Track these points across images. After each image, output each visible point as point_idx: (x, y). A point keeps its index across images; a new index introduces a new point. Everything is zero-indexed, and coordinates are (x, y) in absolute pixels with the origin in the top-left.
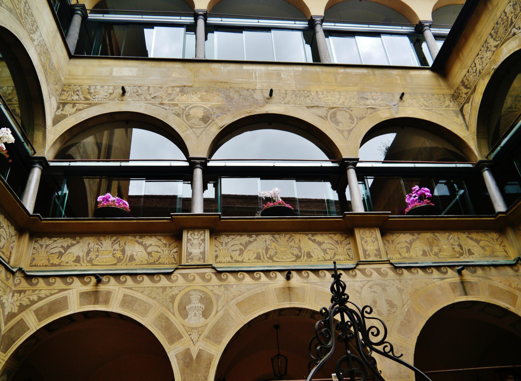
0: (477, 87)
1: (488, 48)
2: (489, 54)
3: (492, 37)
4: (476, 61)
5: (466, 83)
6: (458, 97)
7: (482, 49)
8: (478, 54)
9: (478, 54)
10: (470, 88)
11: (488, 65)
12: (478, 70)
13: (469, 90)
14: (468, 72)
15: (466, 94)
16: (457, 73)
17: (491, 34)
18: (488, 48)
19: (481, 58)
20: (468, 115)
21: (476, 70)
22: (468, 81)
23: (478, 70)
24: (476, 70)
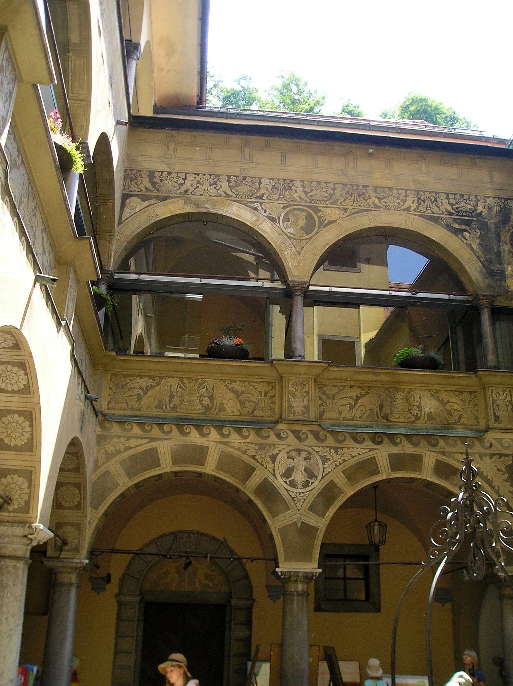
0: (170, 200)
1: (215, 183)
2: (212, 191)
3: (229, 181)
4: (190, 177)
5: (157, 180)
6: (131, 180)
7: (207, 176)
8: (198, 174)
9: (198, 174)
10: (157, 190)
11: (202, 198)
12: (184, 188)
13: (153, 189)
14: (170, 173)
15: (147, 190)
16: (151, 157)
17: (229, 177)
18: (215, 183)
19: (198, 182)
20: (133, 212)
21: (182, 184)
22: (161, 181)
23: (184, 188)
24: (182, 184)
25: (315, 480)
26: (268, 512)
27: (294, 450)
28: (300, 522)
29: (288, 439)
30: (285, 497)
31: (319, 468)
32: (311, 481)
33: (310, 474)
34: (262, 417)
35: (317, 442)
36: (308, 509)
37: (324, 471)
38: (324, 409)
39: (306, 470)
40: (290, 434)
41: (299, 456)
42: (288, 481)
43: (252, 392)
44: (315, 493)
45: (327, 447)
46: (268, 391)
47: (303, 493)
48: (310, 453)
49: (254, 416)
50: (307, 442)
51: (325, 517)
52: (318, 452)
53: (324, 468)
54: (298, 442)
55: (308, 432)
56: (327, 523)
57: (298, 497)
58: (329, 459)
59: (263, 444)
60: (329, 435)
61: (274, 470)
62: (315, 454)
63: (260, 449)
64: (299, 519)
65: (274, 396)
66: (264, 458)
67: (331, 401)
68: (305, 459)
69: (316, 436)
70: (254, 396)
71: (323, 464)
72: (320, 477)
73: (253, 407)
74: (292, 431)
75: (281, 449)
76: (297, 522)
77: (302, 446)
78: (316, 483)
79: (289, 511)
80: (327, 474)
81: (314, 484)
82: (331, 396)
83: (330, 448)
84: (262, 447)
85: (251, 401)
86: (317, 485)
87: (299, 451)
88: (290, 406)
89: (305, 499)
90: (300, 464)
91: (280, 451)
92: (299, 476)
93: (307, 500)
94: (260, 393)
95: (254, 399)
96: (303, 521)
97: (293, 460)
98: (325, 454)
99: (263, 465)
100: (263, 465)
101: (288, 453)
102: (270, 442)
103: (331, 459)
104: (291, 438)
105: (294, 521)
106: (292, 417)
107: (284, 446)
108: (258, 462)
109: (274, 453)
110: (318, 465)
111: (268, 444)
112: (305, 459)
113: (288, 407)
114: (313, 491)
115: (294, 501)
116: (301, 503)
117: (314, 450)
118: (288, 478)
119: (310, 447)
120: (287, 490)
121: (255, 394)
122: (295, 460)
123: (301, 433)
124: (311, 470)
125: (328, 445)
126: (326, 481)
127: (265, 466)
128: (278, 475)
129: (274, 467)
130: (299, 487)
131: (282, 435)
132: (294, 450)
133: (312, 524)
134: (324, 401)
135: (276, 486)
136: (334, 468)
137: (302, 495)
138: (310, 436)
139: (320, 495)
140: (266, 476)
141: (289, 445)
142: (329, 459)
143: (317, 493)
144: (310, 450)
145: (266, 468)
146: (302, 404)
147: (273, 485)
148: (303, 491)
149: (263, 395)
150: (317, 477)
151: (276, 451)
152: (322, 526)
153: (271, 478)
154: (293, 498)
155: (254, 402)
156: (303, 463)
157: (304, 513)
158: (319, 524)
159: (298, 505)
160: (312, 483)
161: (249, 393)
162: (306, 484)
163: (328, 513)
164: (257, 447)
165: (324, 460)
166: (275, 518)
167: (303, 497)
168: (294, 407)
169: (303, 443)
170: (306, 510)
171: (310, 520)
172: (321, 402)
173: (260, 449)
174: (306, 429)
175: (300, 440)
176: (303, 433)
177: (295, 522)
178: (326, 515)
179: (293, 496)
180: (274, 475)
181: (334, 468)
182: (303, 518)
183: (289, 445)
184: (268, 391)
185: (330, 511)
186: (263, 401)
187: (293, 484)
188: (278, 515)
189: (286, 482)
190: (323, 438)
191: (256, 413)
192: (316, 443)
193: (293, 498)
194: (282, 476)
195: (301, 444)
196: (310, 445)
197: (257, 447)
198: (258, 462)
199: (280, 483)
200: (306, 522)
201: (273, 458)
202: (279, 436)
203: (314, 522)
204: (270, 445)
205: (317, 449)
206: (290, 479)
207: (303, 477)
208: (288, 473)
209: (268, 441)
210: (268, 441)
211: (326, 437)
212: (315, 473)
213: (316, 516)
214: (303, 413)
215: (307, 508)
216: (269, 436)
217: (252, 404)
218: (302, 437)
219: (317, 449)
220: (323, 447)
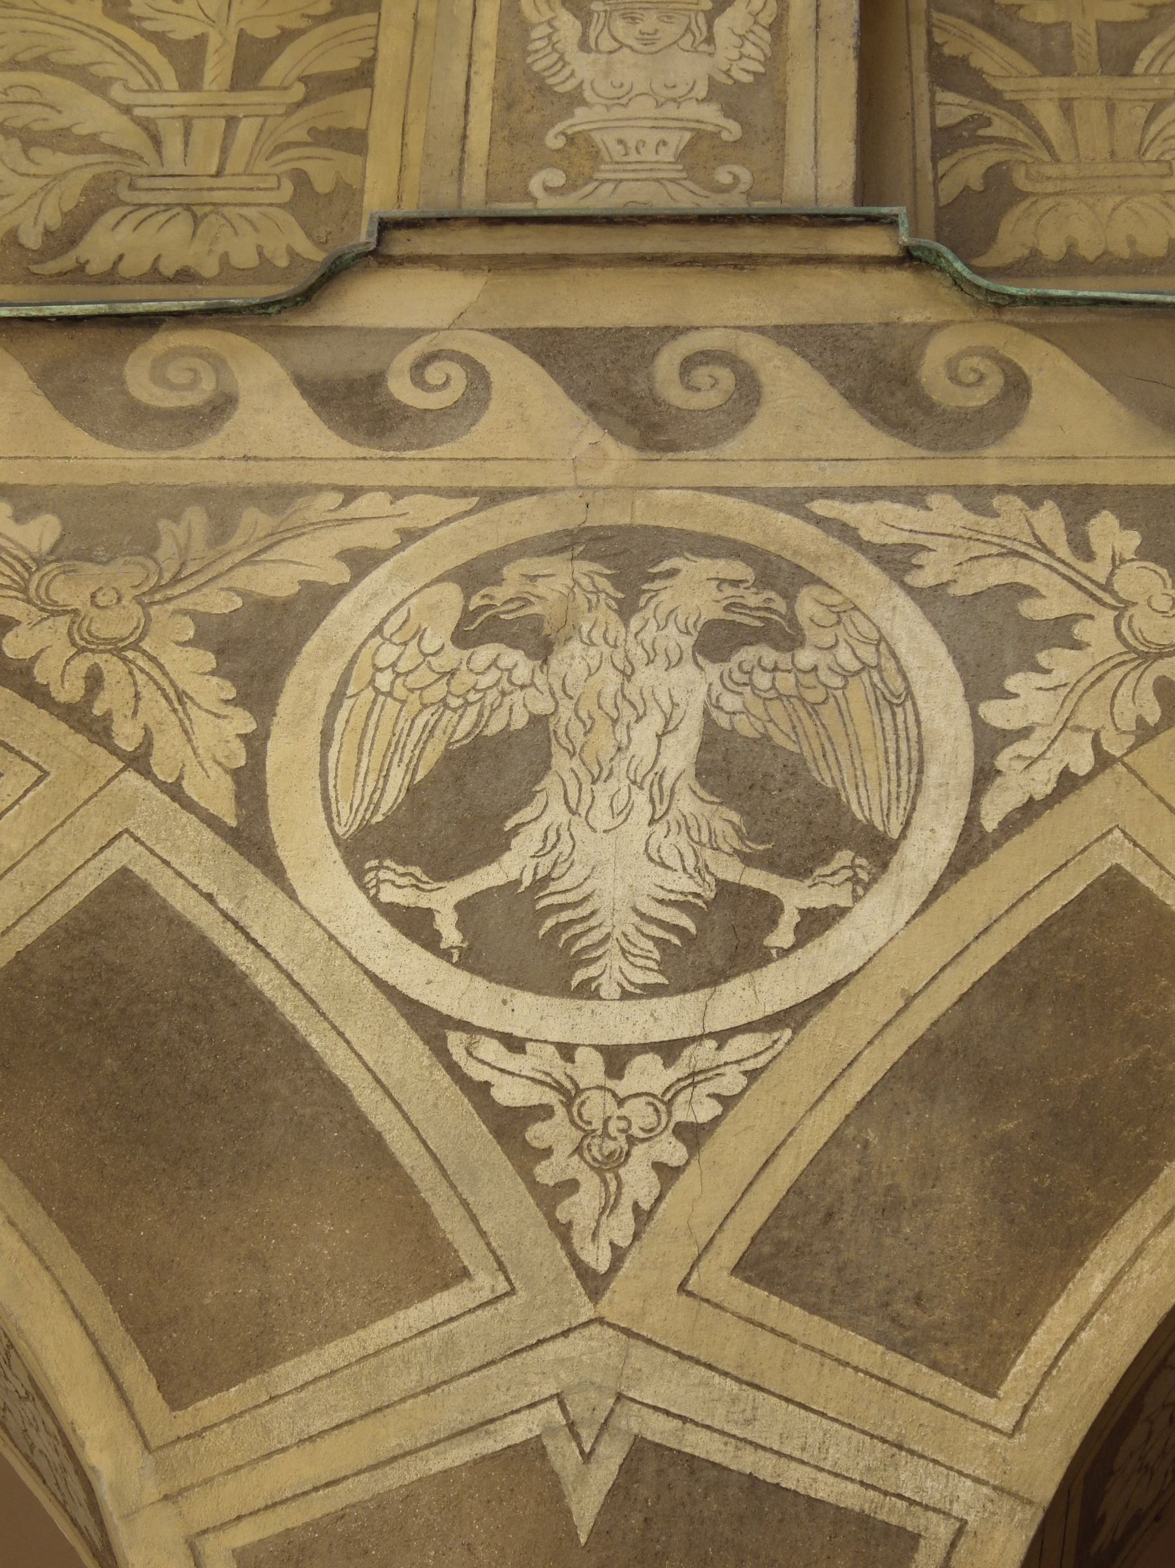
25: (861, 887)
26: (101, 1311)
27: (565, 543)
28: (612, 1456)
29: (486, 434)
30: (381, 1116)
31: (916, 724)
32: (796, 896)
33: (789, 817)
34: (185, 276)
35: (881, 443)
36: (752, 1267)
37: (984, 776)
38: (997, 177)
39: (725, 765)
40: (517, 376)
41: (626, 610)
42: (444, 901)
43: (85, 50)
44: (864, 1044)
45: (1033, 496)
46: (287, 36)
47: (669, 1051)
48: (780, 574)
49: (78, 274)
50: (752, 454)
51: (1025, 1367)
52: (896, 561)
53: (989, 743)
54: (618, 457)
55: (755, 350)
56: (1044, 1467)
57: (596, 1107)
58: (1061, 632)
59: (121, 495)
60: (1049, 367)
61: (250, 782)
62: (864, 582)
63: (70, 554)
64: (589, 1406)
65: (362, 76)
66: (117, 648)
67: (1090, 88)
68: (717, 641)
69: (879, 381)
70: (99, 86)
71: (981, 681)
72: (929, 846)
73: (71, 194)
74: (547, 347)
75: (381, 536)
76: (564, 1456)
77: (670, 493)
78: (875, 921)
79: (445, 1303)
80: (1030, 811)
81: (838, 936)
82: (1087, 47)
83: (1079, 502)
84: (102, 527)
85: (60, 139)
86: (892, 947)
87: (631, 560)
88: (528, 99)
89: (693, 1136)
90: (641, 699)
91: (362, 562)
92: (620, 846)
93: (736, 1150)
94: (188, 58)
95: (92, 115)
96: (659, 1429)
97: (542, 648)
98: (1000, 573)
99: (99, 731)
100: (99, 731)
101: (474, 575)
102: (224, 475)
103: (1098, 632)
104: (535, 424)
105: (518, 1431)
106: (544, 190)
107: (420, 510)
108: (37, 694)
109: (277, 580)
110: (897, 699)
111: (200, 494)
112: (717, 641)
113: (506, 101)
114: (819, 1024)
115: (524, 1157)
116: (639, 1181)
117: (846, 533)
118: (444, 868)
119: (793, 502)
120: (432, 1026)
121: (113, 66)
122: (572, 660)
123: (667, 362)
124: (795, 769)
125: (1040, 474)
126: (1027, 888)
127: (127, 736)
128: (302, 832)
129: (255, 744)
130: (611, 971)
131: (401, 388)
132: (565, 543)
133: (794, 1478)
134: (993, 96)
135: (265, 980)
136: (1145, 733)
137: (648, 1074)
138: (790, 382)
139: (936, 1064)
140: (120, 856)
141: (493, 497)
142: (1061, 632)
143: (894, 1047)
144: (788, 533)
145: (138, 762)
146: (689, 69)
147: (221, 965)
148: (673, 1017)
149: (216, 69)
150: (880, 850)
151: (311, 559)
152: (966, 1497)
153: (192, 875)
154: (509, 1125)
155: (91, 143)
156: (689, 687)
157: (667, 1317)
158: (909, 1477)
159: (581, 1208)
160: (816, 923)
161: (43, 64)
162: (721, 937)
163: (1060, 1318)
164: (42, 532)
165: (992, 639)
166: (210, 1407)
167: (666, 1101)
168: (576, 99)
169: (693, 467)
170: (716, 1276)
171: (775, 1422)
172: (954, 107)
173: (70, 554)
174: (724, 310)
175: (650, 427)
176: (688, 364)
177: (531, 1453)
178: (1044, 1340)
179: (509, 1093)
180: (250, 839)
181: (1145, 733)
182: (664, 1385)
183: (493, 497)
184: (287, 36)
185: (1092, 1280)
186: (208, 131)
187: (528, 944)
188: (258, 1357)
189: (415, 925)
190: (979, 398)
191: (102, 245)
192: (868, 450)
193: (509, 1125)
194: (361, 850)
195: (666, 468)
196: (784, 477)
197: (42, 532)
198: (37, 694)
199: (328, 941)
200: (699, 1444)
201: (256, 652)
202: (356, 404)
203: (842, 1450)
204: (222, 505)
205: (880, 522)
206: (489, 877)
207: (671, 845)
208: (457, 808)
209: (201, 462)
210: (201, 462)
211: (1017, 387)
212: (866, 804)
213: (861, 1349)
214: (701, 151)
215: (732, 1247)
216: (221, 407)
217: (62, 161)
218: (675, 394)
219: (880, 522)
220: (977, 498)
